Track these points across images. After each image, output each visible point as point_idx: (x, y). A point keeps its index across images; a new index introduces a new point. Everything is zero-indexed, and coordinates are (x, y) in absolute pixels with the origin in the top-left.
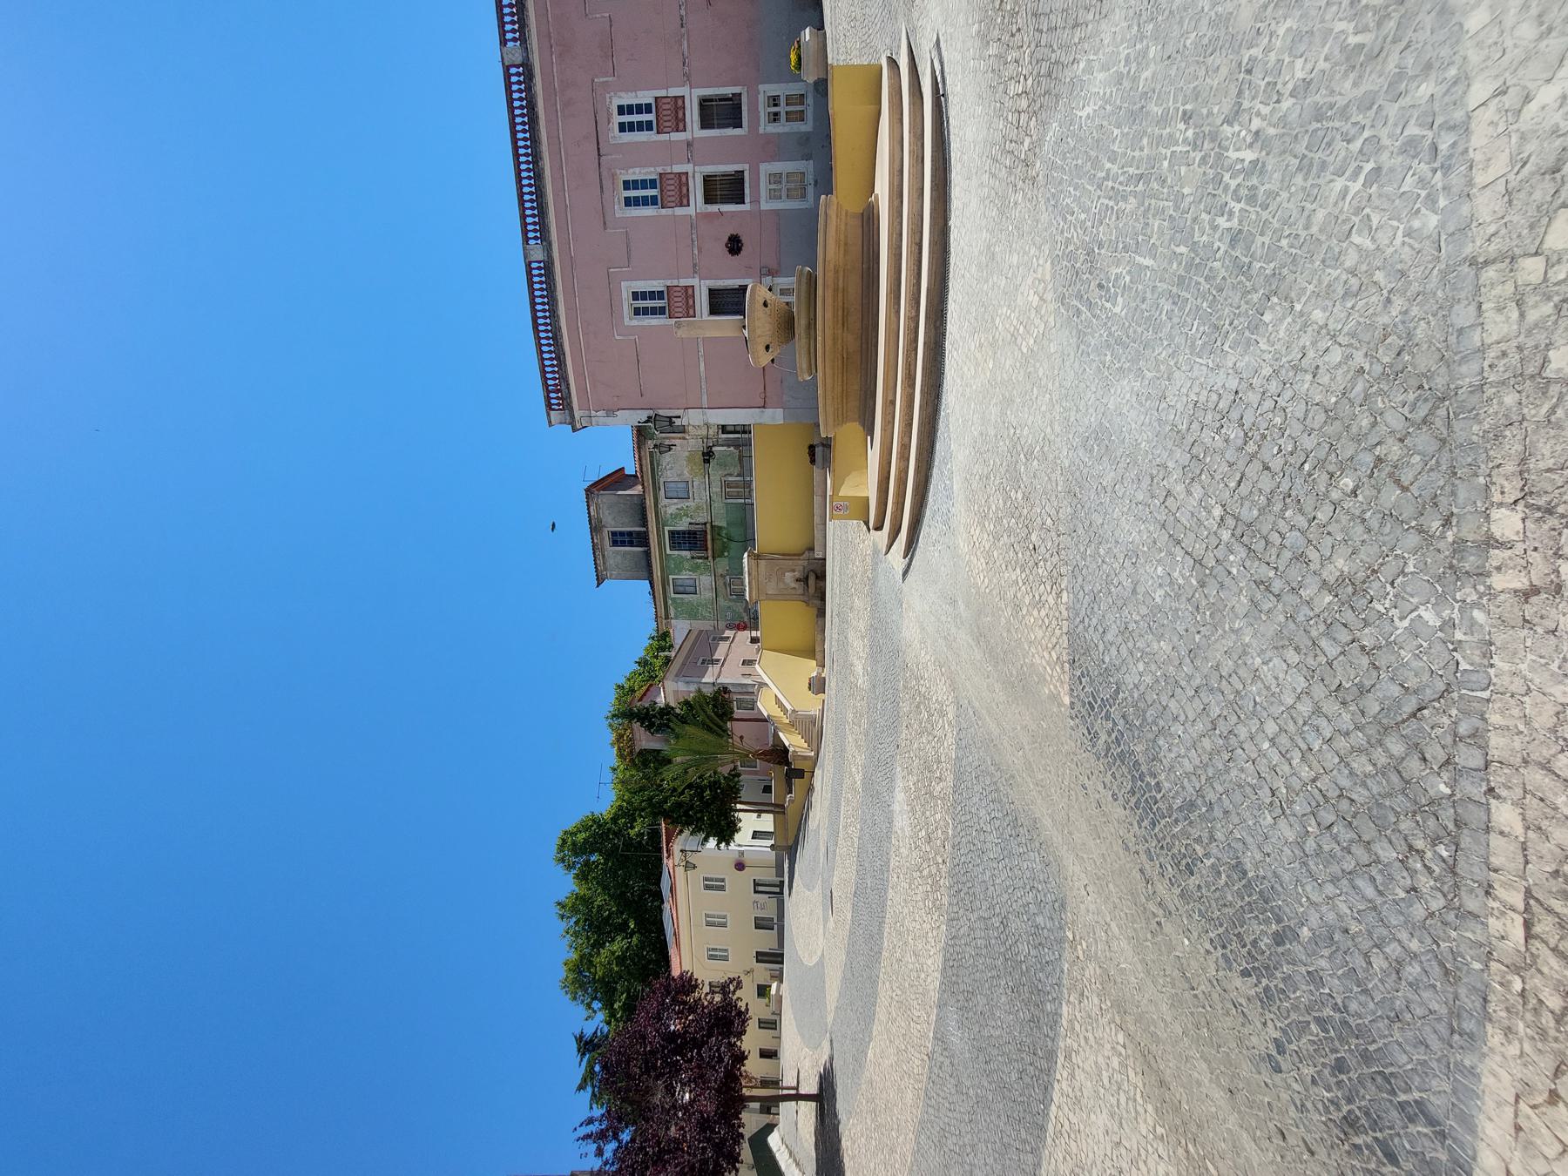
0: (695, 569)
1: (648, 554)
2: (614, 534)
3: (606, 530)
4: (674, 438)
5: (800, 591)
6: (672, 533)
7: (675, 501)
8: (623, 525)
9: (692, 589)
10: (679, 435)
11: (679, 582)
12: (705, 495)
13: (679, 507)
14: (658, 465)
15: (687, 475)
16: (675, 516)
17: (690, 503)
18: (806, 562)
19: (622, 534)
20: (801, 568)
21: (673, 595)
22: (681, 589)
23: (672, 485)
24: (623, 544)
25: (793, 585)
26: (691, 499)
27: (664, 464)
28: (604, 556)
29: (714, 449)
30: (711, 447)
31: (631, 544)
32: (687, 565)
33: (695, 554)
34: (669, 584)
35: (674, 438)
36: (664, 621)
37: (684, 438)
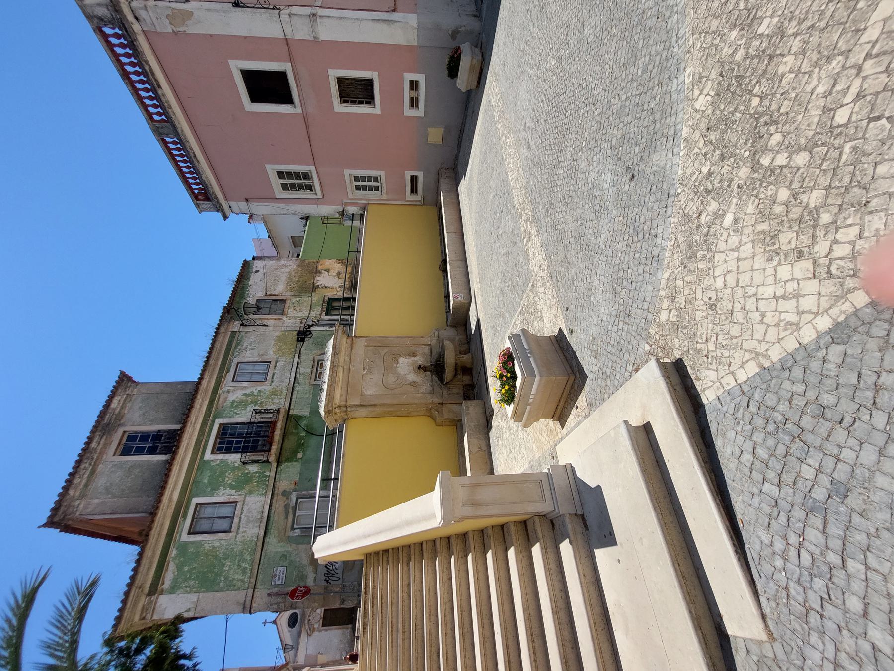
0: (243, 482)
1: (169, 464)
2: (132, 437)
3: (120, 431)
4: (267, 319)
5: (426, 387)
6: (224, 428)
7: (245, 384)
8: (153, 422)
9: (224, 525)
10: (275, 317)
11: (208, 511)
12: (289, 378)
13: (248, 391)
14: (238, 345)
15: (271, 355)
16: (240, 404)
17: (266, 387)
18: (434, 342)
19: (145, 437)
20: (426, 350)
21: (185, 537)
22: (204, 525)
23: (249, 368)
24: (139, 451)
25: (412, 377)
26: (268, 382)
27: (246, 344)
28: (93, 472)
29: (312, 328)
30: (310, 326)
31: (152, 451)
32: (230, 478)
33: (248, 457)
34: (185, 516)
35: (267, 319)
36: (143, 601)
37: (279, 319)
